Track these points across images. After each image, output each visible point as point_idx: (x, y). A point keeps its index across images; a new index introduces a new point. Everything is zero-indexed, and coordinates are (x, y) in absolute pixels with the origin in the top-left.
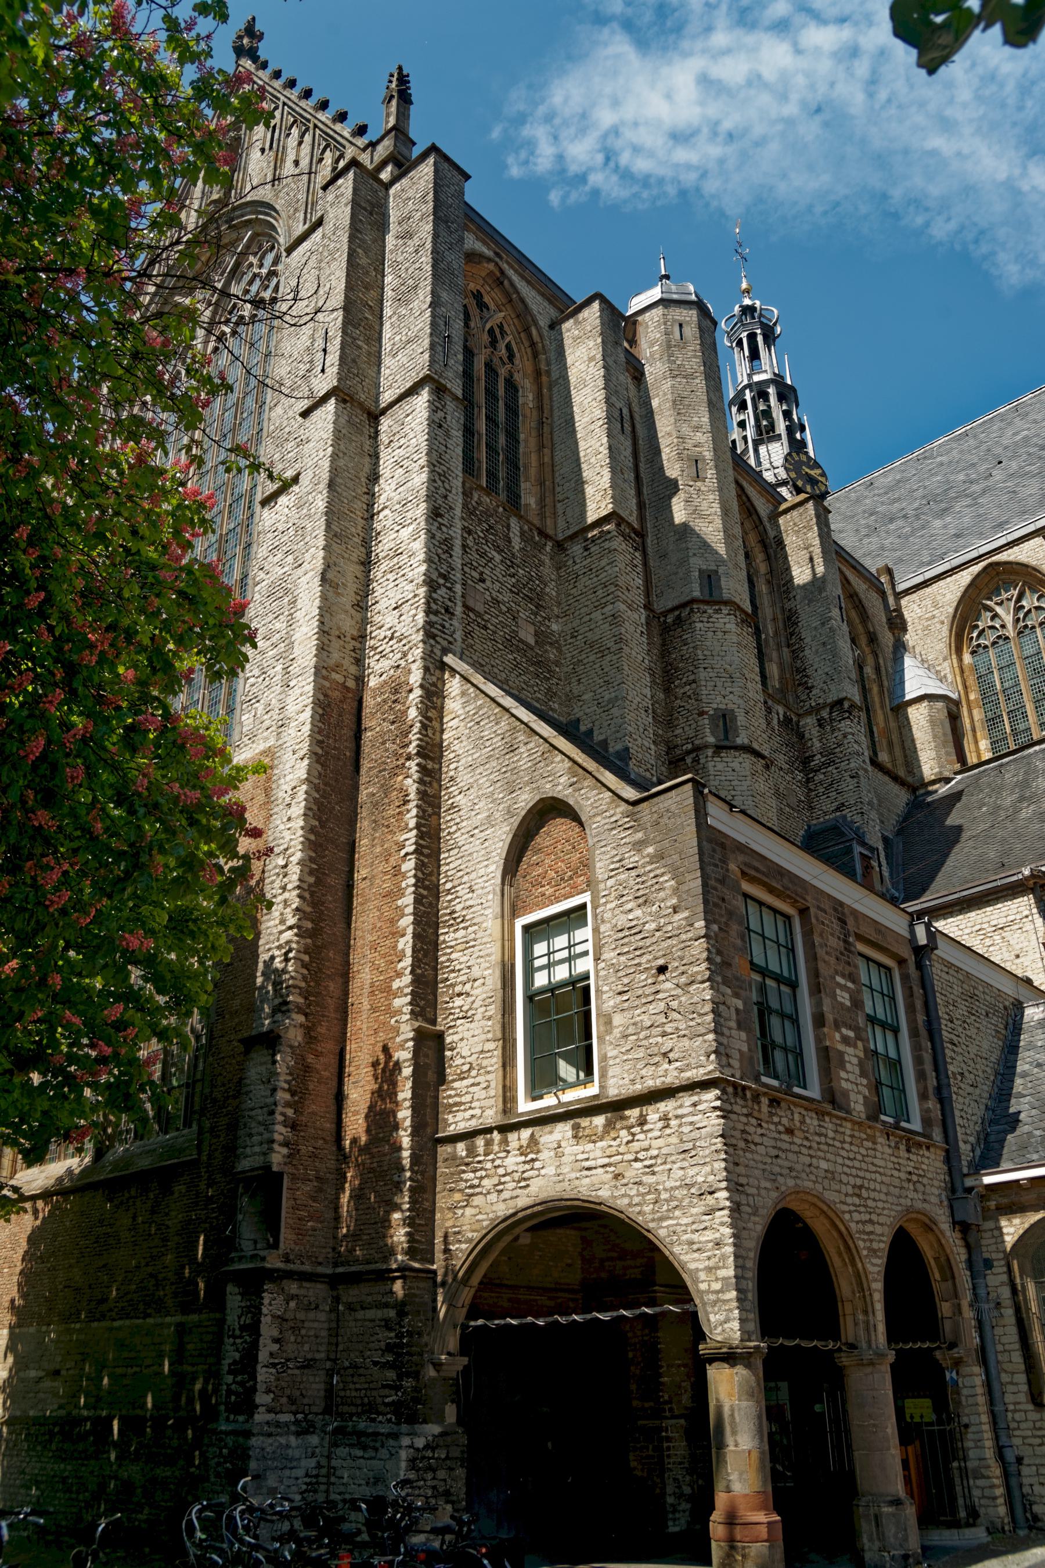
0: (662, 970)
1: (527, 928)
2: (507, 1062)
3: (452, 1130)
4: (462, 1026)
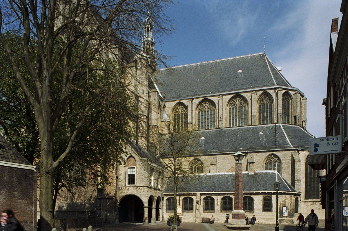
0: (143, 176)
1: (128, 168)
2: (126, 181)
3: (119, 186)
4: (120, 176)
